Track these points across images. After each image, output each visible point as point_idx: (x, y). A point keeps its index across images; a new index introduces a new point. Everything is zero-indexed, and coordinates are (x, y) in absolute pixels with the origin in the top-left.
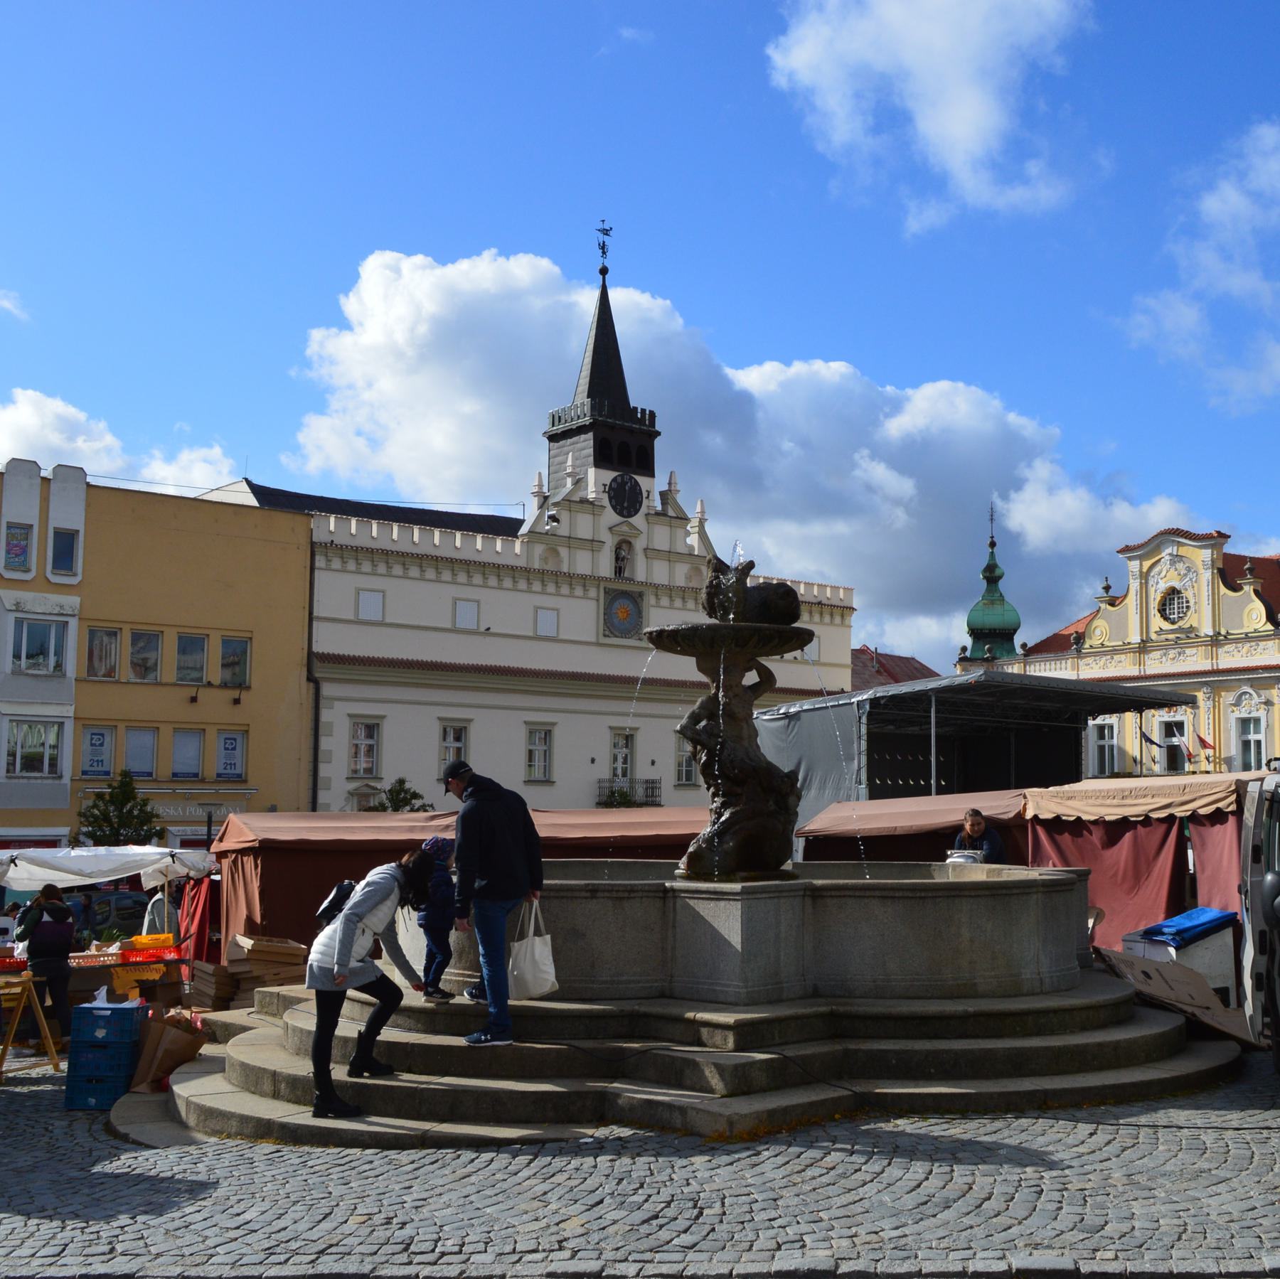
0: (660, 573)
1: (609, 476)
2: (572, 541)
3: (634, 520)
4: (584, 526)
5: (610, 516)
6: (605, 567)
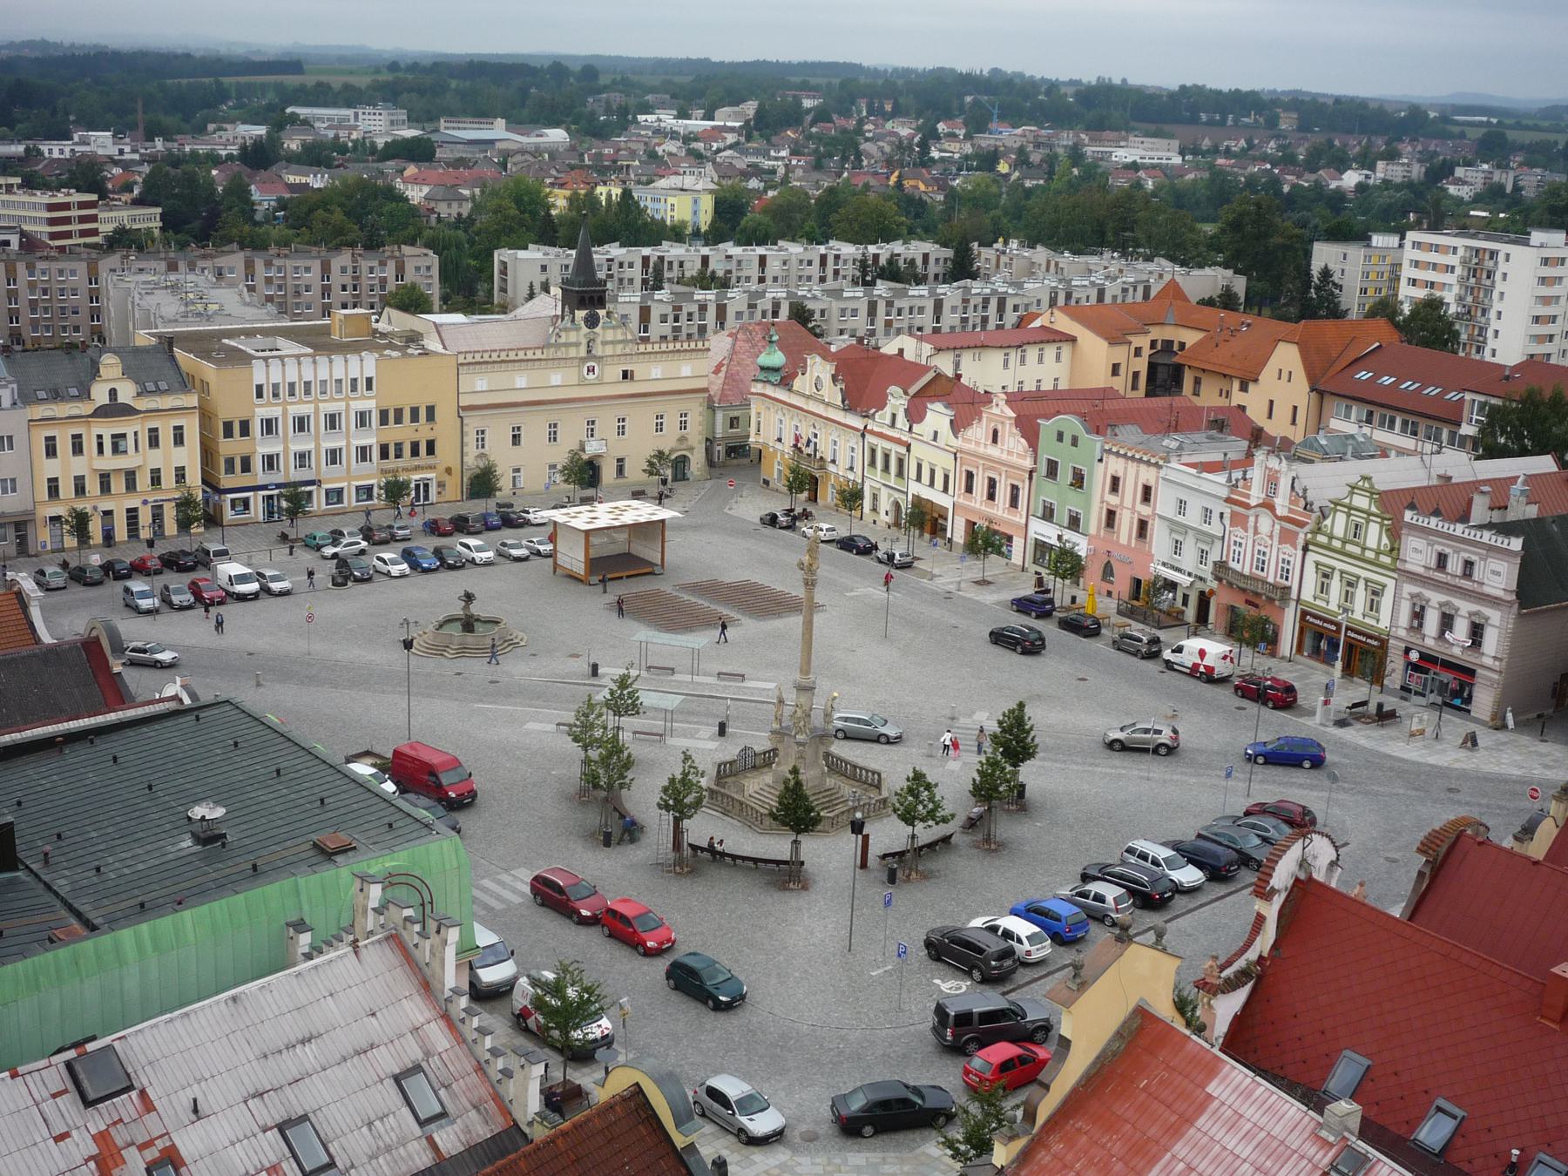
0: (609, 350)
2: (567, 345)
3: (596, 330)
4: (573, 337)
5: (585, 330)
6: (583, 352)
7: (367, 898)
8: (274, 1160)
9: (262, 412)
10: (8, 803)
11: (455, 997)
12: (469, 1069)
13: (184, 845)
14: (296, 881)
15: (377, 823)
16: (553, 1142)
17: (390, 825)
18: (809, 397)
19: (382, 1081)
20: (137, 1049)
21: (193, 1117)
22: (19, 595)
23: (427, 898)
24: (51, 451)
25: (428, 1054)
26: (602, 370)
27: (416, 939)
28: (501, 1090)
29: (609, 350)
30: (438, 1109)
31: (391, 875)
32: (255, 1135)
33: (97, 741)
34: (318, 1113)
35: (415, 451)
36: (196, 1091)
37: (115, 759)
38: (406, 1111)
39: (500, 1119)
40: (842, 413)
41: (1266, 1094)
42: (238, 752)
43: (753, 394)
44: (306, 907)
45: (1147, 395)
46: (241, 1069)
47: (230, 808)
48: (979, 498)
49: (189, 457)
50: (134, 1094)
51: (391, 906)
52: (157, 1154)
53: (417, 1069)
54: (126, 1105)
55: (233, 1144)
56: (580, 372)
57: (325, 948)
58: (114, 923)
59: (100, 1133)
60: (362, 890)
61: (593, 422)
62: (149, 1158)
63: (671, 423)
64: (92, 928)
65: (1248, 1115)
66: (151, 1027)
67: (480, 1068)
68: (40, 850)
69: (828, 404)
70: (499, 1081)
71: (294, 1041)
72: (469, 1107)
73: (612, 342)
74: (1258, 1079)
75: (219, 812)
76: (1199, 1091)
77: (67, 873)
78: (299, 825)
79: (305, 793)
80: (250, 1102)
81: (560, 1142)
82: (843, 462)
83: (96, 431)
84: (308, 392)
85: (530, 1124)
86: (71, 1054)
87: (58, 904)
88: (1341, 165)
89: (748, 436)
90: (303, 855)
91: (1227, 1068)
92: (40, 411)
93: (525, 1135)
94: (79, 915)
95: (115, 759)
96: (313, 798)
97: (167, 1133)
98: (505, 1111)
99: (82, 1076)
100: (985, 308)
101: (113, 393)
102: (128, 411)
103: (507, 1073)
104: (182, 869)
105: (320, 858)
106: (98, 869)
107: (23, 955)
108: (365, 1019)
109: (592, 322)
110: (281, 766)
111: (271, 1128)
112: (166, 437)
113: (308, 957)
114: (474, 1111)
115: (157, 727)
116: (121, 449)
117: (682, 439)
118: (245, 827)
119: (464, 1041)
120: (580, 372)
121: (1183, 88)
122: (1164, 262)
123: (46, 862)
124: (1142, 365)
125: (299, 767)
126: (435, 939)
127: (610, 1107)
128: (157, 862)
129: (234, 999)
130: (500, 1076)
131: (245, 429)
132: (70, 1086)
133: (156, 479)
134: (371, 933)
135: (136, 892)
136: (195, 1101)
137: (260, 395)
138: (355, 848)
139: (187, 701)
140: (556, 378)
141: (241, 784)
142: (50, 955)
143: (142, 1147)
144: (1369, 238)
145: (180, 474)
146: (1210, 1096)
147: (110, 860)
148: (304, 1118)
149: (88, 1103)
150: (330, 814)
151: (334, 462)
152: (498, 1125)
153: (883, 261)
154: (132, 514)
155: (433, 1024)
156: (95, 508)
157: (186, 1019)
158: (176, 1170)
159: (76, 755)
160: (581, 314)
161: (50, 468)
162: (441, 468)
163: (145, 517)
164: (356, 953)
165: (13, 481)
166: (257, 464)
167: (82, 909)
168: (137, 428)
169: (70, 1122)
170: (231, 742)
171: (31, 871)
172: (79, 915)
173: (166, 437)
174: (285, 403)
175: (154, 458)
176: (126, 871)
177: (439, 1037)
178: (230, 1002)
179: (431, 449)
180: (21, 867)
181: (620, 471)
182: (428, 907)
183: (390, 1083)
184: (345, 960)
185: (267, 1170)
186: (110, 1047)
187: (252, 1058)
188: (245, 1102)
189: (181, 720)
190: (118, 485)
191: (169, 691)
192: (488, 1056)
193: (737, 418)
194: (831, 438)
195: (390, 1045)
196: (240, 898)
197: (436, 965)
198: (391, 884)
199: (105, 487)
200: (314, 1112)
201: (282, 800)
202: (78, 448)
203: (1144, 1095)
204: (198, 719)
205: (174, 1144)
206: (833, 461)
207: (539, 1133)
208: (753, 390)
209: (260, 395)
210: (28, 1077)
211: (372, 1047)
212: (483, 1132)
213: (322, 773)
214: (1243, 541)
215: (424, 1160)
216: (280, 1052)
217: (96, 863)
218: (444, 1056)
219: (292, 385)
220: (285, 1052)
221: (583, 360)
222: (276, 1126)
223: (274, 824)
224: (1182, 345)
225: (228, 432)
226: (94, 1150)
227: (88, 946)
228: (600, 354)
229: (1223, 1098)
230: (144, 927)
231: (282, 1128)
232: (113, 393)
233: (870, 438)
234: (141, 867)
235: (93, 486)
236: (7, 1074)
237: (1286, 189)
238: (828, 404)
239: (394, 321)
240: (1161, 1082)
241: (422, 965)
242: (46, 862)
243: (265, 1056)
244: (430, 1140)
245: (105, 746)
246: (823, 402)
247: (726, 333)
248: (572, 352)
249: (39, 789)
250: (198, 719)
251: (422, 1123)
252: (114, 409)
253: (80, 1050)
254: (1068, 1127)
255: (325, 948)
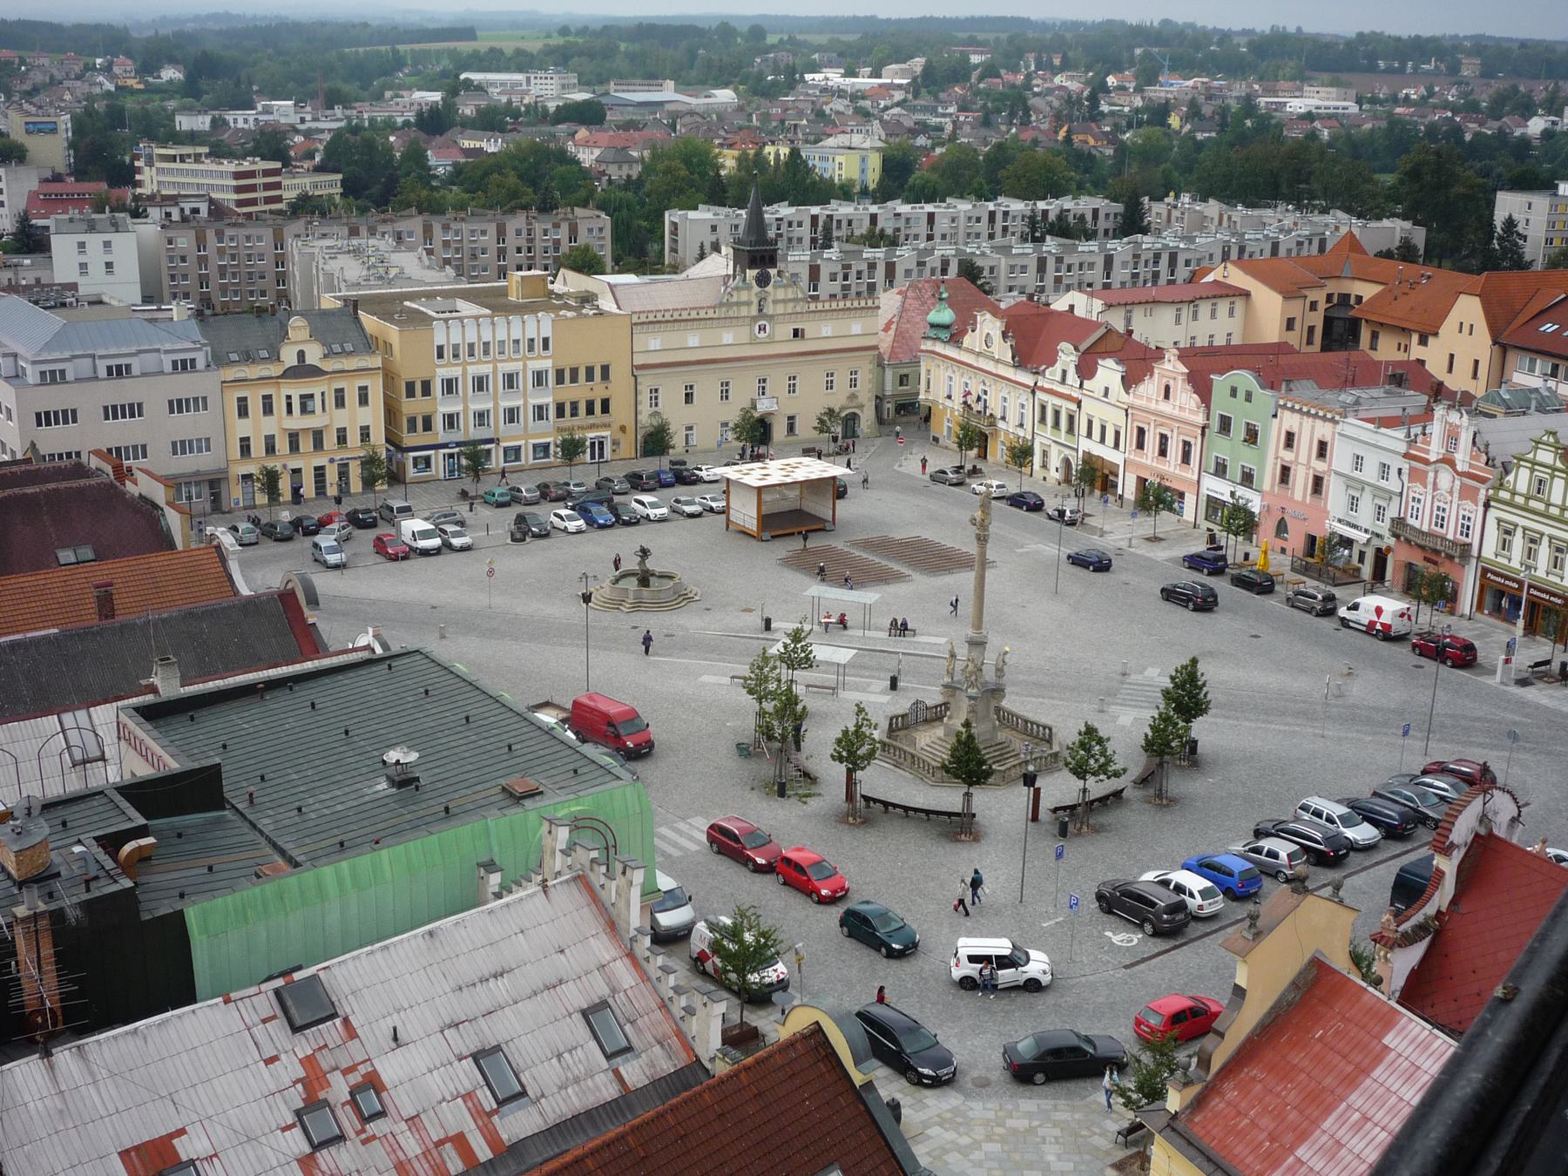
0: (780, 309)
1: (754, 272)
2: (738, 304)
4: (744, 296)
5: (756, 289)
6: (754, 311)
7: (555, 839)
8: (470, 1088)
9: (443, 372)
10: (214, 746)
11: (639, 936)
12: (654, 1006)
13: (379, 787)
14: (486, 824)
15: (562, 770)
16: (736, 1075)
17: (575, 771)
18: (979, 354)
19: (570, 1015)
20: (340, 978)
21: (393, 1045)
22: (218, 547)
23: (611, 842)
24: (243, 411)
25: (614, 991)
26: (772, 329)
27: (603, 880)
28: (684, 1027)
29: (780, 309)
30: (624, 1043)
31: (576, 819)
32: (451, 1064)
33: (296, 688)
34: (510, 1044)
35: (590, 410)
36: (395, 1020)
37: (313, 705)
38: (593, 1044)
39: (684, 1055)
40: (1012, 370)
41: (1444, 1047)
42: (428, 700)
43: (922, 351)
44: (496, 849)
45: (1325, 348)
46: (437, 1000)
47: (423, 753)
48: (1150, 455)
49: (373, 416)
50: (338, 1021)
51: (578, 848)
52: (360, 1079)
53: (603, 1005)
54: (331, 1031)
55: (430, 1071)
56: (752, 331)
57: (514, 888)
58: (314, 860)
59: (307, 1057)
60: (550, 832)
61: (764, 381)
62: (352, 1082)
63: (841, 380)
64: (297, 865)
65: (1425, 1067)
66: (354, 958)
67: (664, 1006)
68: (245, 790)
69: (998, 361)
70: (682, 1018)
71: (487, 976)
72: (653, 1041)
73: (785, 301)
74: (1436, 1031)
75: (413, 757)
76: (1376, 1041)
77: (270, 812)
78: (487, 770)
79: (492, 740)
80: (446, 1032)
81: (743, 1075)
82: (1013, 418)
83: (285, 391)
84: (486, 352)
85: (712, 1060)
86: (280, 982)
87: (262, 840)
88: (1527, 110)
89: (918, 394)
90: (493, 799)
91: (1405, 1020)
92: (231, 373)
93: (707, 1070)
94: (282, 852)
95: (313, 705)
96: (500, 744)
97: (369, 1059)
98: (688, 1047)
99: (289, 1003)
100: (1156, 263)
101: (301, 355)
102: (315, 372)
103: (690, 1011)
104: (378, 811)
105: (508, 802)
106: (299, 809)
107: (233, 889)
108: (555, 956)
109: (763, 281)
110: (470, 713)
111: (466, 1058)
112: (352, 397)
113: (498, 896)
114: (658, 1047)
115: (352, 675)
116: (309, 409)
117: (853, 397)
118: (437, 771)
119: (649, 979)
120: (752, 331)
121: (1361, 35)
122: (1340, 214)
123: (251, 802)
124: (1317, 320)
125: (487, 715)
126: (620, 880)
127: (791, 1044)
128: (355, 803)
129: (431, 933)
130: (683, 1013)
131: (427, 389)
132: (279, 1013)
133: (342, 438)
134: (559, 873)
135: (336, 832)
136: (395, 1029)
137: (440, 356)
138: (541, 793)
139: (379, 651)
140: (728, 337)
141: (431, 731)
142: (257, 890)
143: (346, 1072)
144: (1556, 187)
145: (365, 433)
146: (1387, 1047)
147: (311, 801)
148: (497, 1048)
149: (296, 1029)
150: (518, 760)
151: (511, 421)
152: (682, 1060)
153: (1052, 217)
154: (320, 472)
155: (618, 962)
156: (285, 466)
157: (386, 952)
158: (378, 1094)
159: (279, 702)
160: (751, 274)
161: (242, 428)
162: (616, 426)
163: (332, 476)
164: (545, 892)
165: (208, 440)
166: (438, 423)
167: (286, 847)
168: (325, 388)
169: (280, 1047)
170: (422, 690)
171: (237, 810)
172: (282, 852)
173: (352, 397)
174: (466, 363)
175: (340, 418)
176: (326, 812)
177: (624, 974)
178: (427, 937)
179: (605, 407)
180: (227, 806)
181: (791, 428)
182: (612, 851)
183: (578, 1017)
184: (535, 899)
185: (463, 1097)
186: (315, 977)
187: (448, 989)
188: (442, 1032)
189: (374, 669)
190: (306, 444)
191: (362, 641)
192: (671, 993)
193: (907, 376)
194: (1002, 394)
195: (578, 981)
196: (434, 838)
197: (621, 905)
198: (577, 828)
199: (294, 447)
200: (506, 1043)
201: (472, 746)
202: (268, 409)
203: (1318, 1047)
204: (390, 667)
205: (375, 1071)
206: (1003, 418)
207: (721, 1068)
208: (923, 347)
209: (440, 356)
210: (239, 1003)
211: (561, 982)
212: (666, 1067)
213: (511, 721)
214: (1422, 498)
215: (610, 1091)
216: (474, 985)
217: (297, 804)
218: (629, 992)
219: (471, 346)
220: (479, 985)
221: (754, 319)
222: (471, 1055)
223: (465, 769)
224: (1359, 299)
225: (411, 392)
226: (301, 1073)
227: (292, 881)
228: (771, 313)
229: (1399, 1050)
230: (344, 865)
231: (476, 1057)
232: (301, 355)
233: (1039, 395)
234: (339, 808)
235: (282, 445)
236: (221, 999)
237: (1468, 137)
238: (998, 361)
239: (569, 282)
240: (1337, 1032)
241: (608, 904)
242: (251, 802)
243: (460, 989)
244: (617, 1073)
245: (305, 693)
246: (993, 359)
247: (895, 290)
248: (744, 311)
249: (243, 733)
250: (390, 667)
251: (608, 1057)
252: (303, 370)
253: (287, 978)
254: (1242, 1075)
255: (514, 888)
